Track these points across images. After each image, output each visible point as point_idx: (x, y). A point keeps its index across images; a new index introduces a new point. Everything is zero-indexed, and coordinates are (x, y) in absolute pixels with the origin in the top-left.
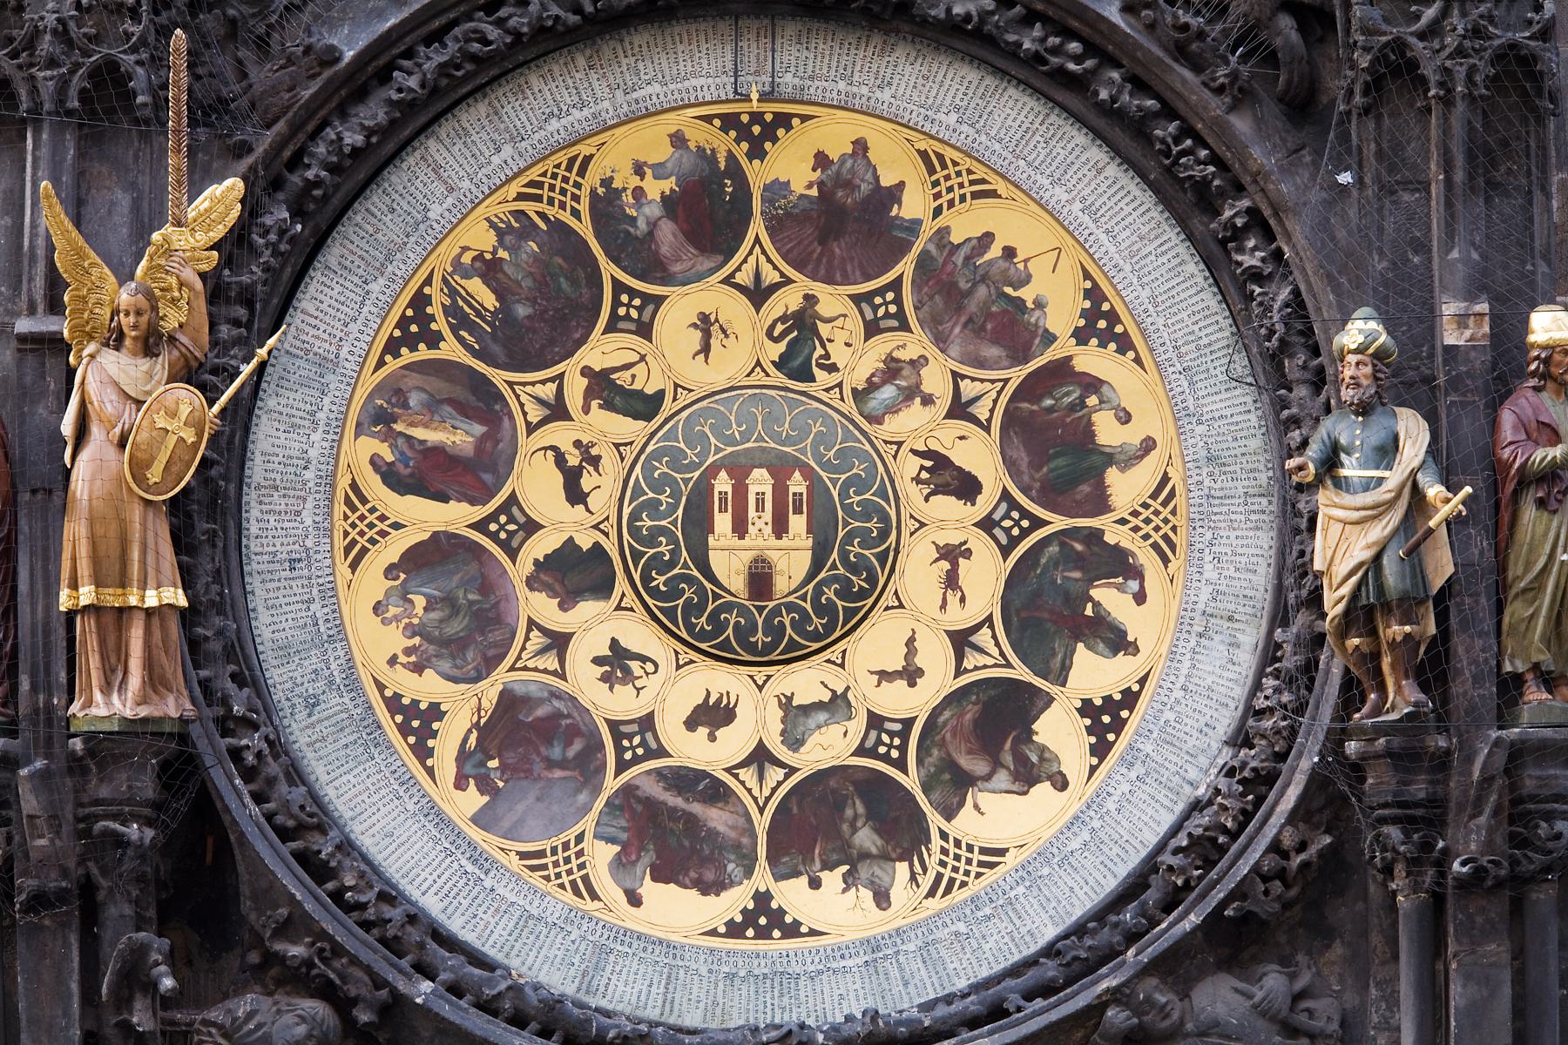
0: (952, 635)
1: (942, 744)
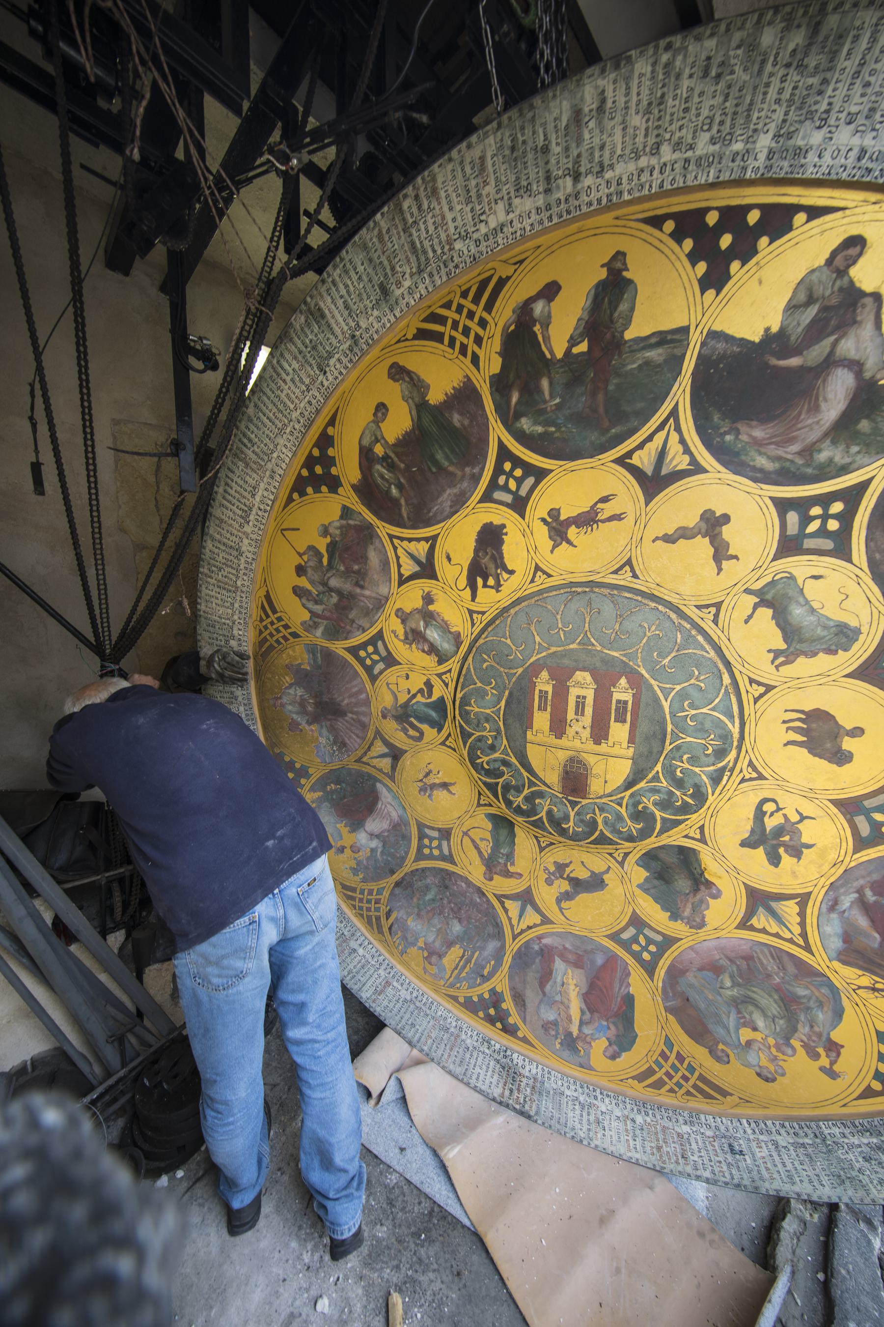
1: (809, 451)
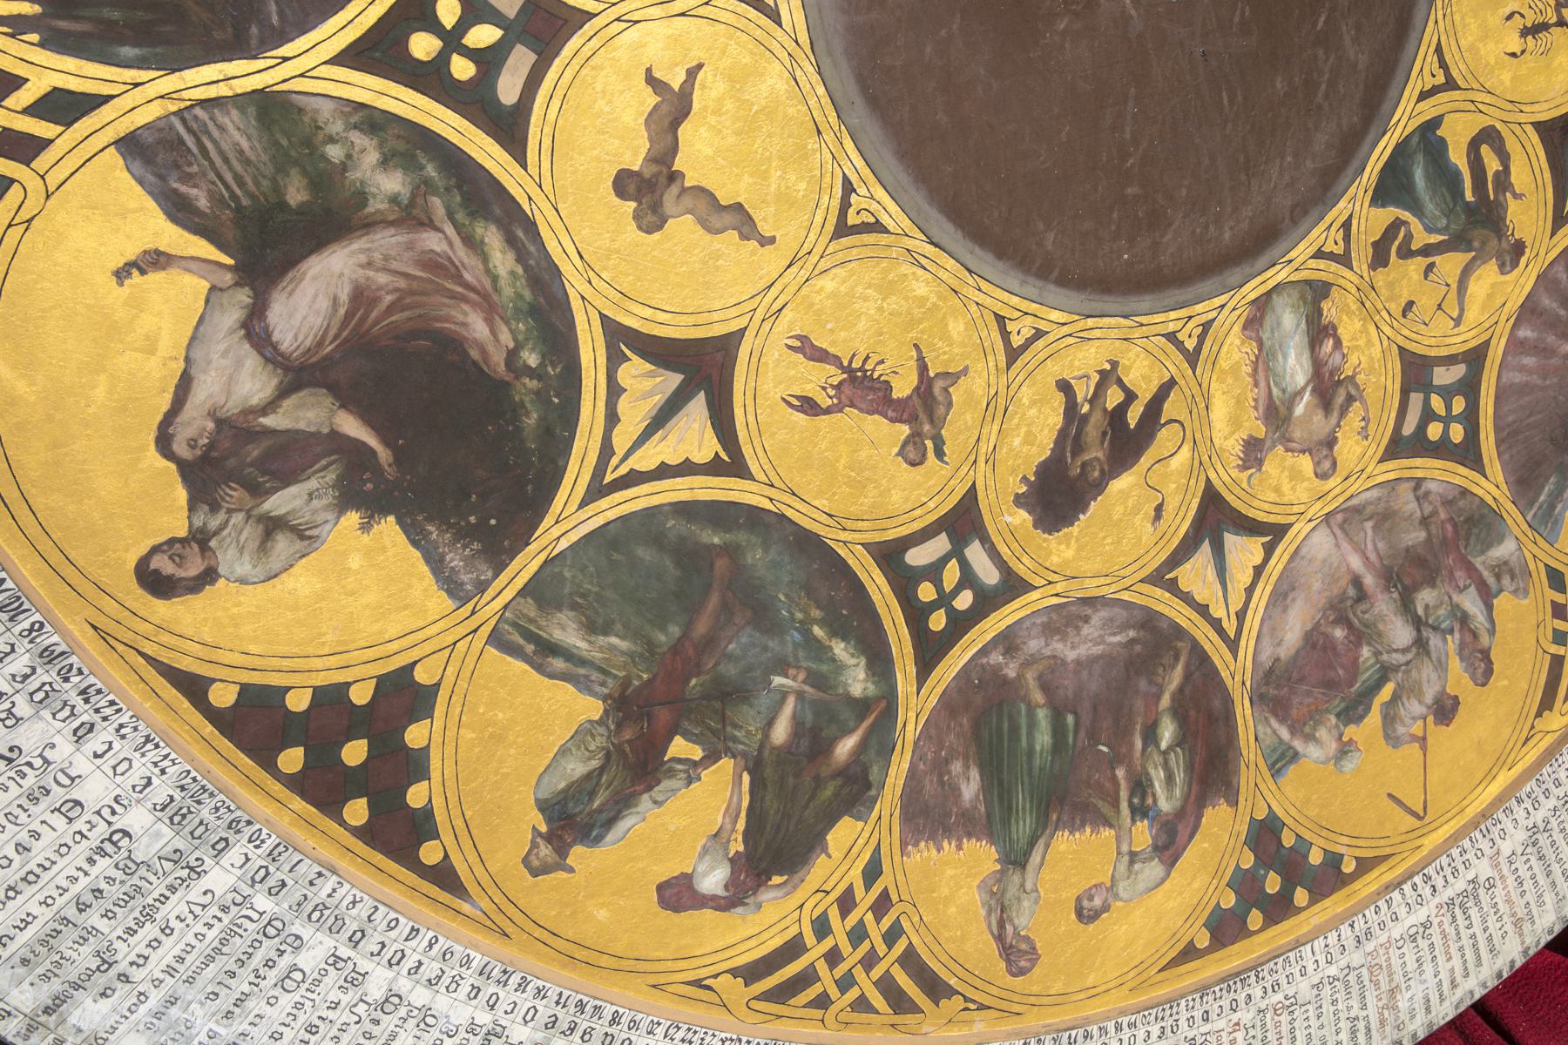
0: (727, 345)
1: (410, 215)
